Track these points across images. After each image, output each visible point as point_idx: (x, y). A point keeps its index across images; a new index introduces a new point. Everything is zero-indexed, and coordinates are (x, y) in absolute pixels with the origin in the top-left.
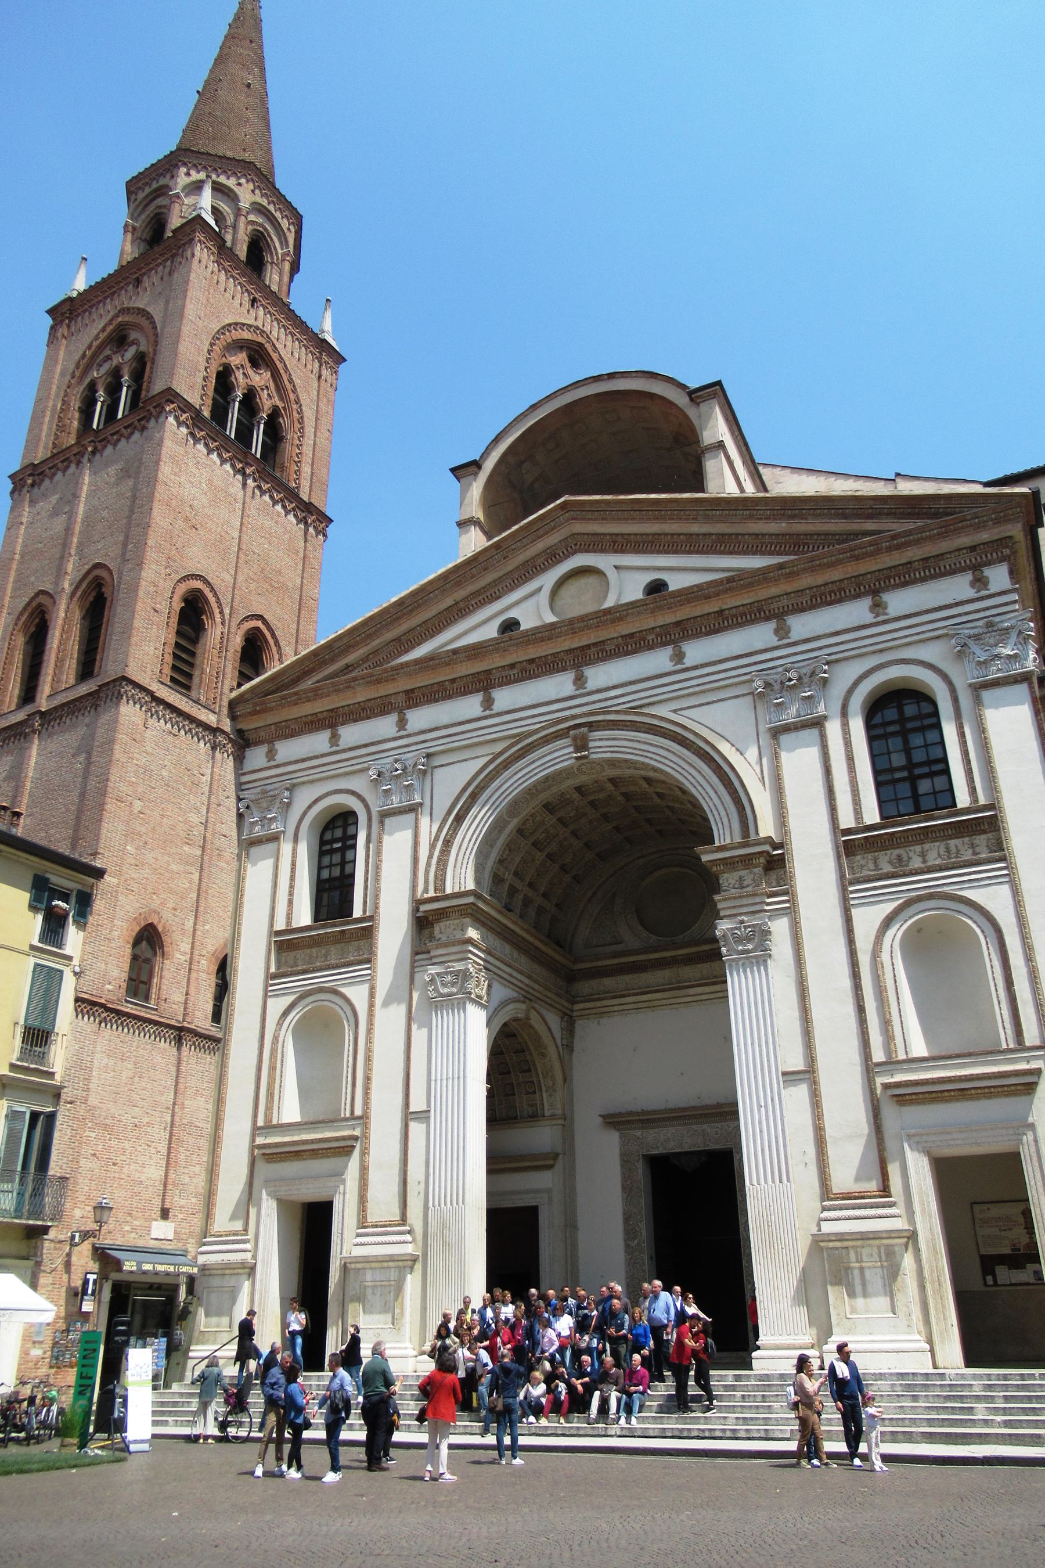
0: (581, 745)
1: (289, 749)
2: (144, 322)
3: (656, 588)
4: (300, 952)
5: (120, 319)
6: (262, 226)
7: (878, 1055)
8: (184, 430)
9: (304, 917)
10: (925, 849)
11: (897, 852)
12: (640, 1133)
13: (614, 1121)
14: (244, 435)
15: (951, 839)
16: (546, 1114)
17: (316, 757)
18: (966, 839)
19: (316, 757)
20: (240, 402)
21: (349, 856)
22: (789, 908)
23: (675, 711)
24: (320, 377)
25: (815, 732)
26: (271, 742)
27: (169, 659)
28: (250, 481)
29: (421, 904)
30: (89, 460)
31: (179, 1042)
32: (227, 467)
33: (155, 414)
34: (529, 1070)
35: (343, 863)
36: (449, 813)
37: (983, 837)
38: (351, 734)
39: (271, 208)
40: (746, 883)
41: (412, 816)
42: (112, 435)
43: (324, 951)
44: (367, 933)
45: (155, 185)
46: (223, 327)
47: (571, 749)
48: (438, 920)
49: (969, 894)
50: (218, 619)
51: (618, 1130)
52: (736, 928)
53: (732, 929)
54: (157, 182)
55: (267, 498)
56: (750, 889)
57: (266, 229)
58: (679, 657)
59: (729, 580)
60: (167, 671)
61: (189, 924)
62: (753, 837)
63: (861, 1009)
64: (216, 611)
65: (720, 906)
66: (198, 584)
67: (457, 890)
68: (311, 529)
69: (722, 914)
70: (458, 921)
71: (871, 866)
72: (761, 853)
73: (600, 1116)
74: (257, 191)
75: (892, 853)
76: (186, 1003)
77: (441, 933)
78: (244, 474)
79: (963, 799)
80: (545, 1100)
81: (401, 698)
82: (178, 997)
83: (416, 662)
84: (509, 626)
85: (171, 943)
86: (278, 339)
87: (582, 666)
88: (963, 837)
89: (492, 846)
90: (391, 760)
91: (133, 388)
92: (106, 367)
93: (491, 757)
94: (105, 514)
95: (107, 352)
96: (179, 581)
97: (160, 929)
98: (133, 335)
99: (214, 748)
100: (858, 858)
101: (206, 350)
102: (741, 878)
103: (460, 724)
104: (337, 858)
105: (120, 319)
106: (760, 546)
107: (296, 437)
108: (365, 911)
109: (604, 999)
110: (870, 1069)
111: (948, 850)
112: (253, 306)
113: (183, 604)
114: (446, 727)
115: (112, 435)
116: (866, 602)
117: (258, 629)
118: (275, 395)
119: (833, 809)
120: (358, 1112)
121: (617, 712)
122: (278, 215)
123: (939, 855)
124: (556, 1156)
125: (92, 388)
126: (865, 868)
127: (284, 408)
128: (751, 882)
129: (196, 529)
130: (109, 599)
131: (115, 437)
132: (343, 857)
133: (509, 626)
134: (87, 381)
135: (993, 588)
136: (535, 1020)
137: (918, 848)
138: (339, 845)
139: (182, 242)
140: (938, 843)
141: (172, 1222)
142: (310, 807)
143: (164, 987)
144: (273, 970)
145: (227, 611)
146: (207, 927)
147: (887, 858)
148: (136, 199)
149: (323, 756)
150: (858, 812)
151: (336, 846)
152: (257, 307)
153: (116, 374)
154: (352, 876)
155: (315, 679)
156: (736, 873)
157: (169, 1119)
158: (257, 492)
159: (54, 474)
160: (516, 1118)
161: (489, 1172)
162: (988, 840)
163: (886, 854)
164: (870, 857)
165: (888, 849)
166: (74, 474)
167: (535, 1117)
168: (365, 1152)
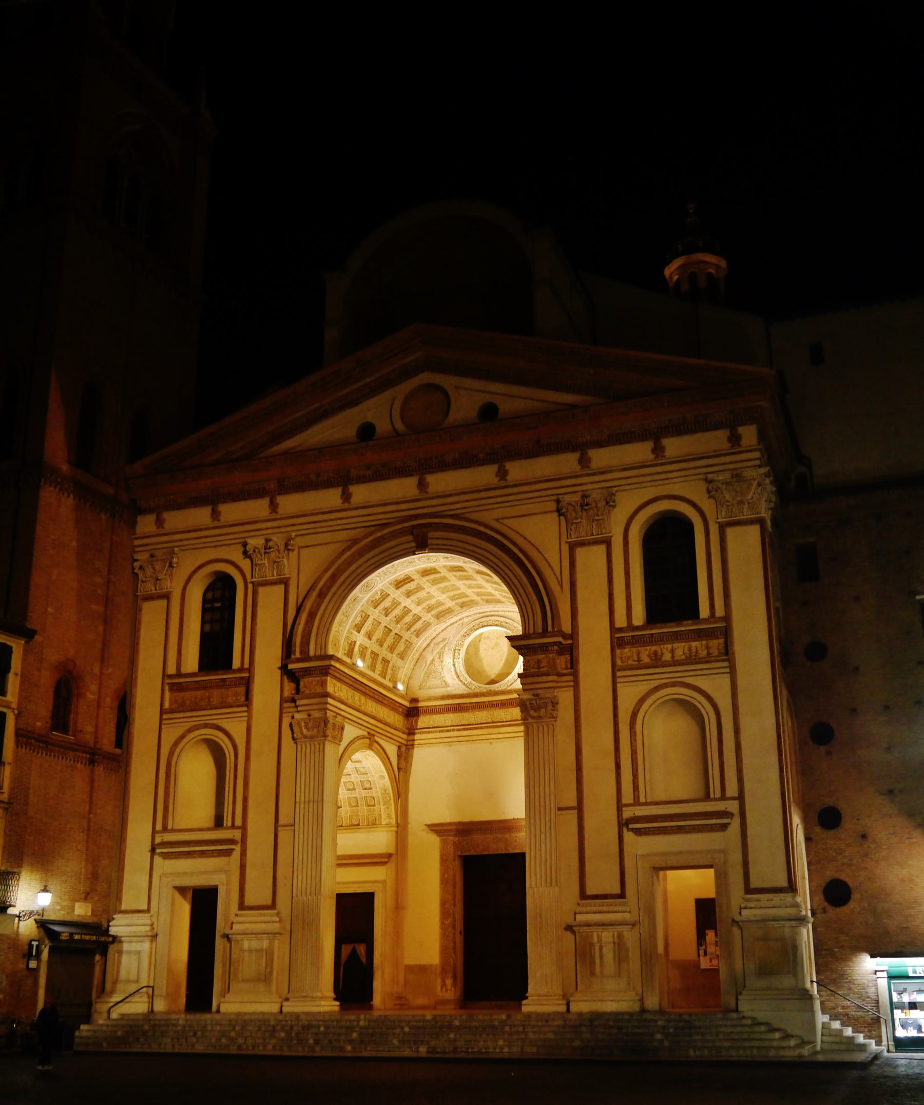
1: (175, 519)
3: (489, 412)
7: (627, 798)
9: (191, 663)
11: (654, 648)
13: (437, 829)
15: (693, 641)
17: (201, 530)
18: (704, 643)
22: (572, 686)
23: (497, 520)
26: (158, 511)
31: (92, 762)
40: (542, 665)
48: (304, 676)
49: (701, 682)
51: (439, 836)
52: (532, 699)
53: (530, 700)
56: (545, 669)
58: (502, 474)
61: (96, 669)
62: (550, 629)
63: (618, 766)
67: (318, 653)
71: (636, 658)
72: (555, 643)
77: (305, 687)
79: (704, 612)
81: (272, 485)
82: (90, 729)
84: (367, 432)
88: (702, 640)
100: (627, 650)
110: (620, 807)
111: (690, 648)
114: (312, 514)
116: (649, 445)
120: (238, 822)
121: (451, 516)
123: (684, 653)
124: (390, 856)
126: (631, 659)
133: (367, 432)
137: (669, 646)
138: (219, 605)
141: (90, 902)
144: (167, 705)
146: (110, 670)
147: (647, 653)
156: (536, 656)
157: (85, 825)
160: (358, 825)
165: (649, 646)
168: (243, 854)
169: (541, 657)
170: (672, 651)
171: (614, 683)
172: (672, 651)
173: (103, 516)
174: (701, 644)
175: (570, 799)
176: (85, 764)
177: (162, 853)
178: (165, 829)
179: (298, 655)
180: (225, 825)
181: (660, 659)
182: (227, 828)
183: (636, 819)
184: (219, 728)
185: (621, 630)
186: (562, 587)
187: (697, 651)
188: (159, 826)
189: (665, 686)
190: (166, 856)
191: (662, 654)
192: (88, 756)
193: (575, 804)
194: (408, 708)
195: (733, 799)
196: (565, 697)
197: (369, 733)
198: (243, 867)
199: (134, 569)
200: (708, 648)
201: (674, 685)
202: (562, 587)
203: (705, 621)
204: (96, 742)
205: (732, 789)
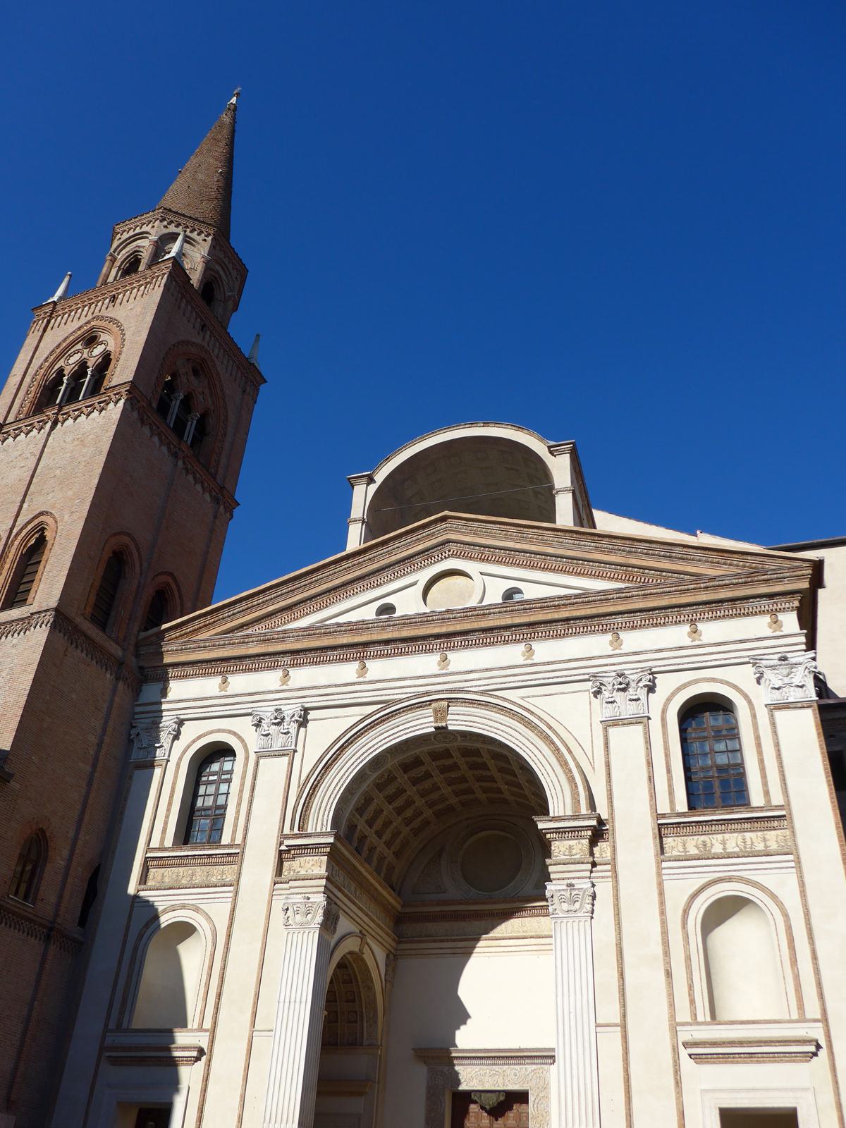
0: (441, 714)
2: (115, 328)
4: (169, 869)
5: (93, 323)
6: (217, 272)
7: (683, 1015)
8: (135, 414)
10: (725, 839)
12: (447, 1069)
14: (179, 428)
16: (364, 1044)
17: (206, 699)
19: (206, 699)
20: (181, 401)
21: (223, 788)
23: (522, 698)
24: (244, 391)
25: (640, 728)
27: (93, 598)
28: (180, 463)
29: (285, 838)
30: (52, 428)
31: (48, 938)
32: (164, 449)
33: (114, 399)
34: (353, 1001)
35: (217, 794)
36: (320, 760)
37: (773, 833)
38: (240, 682)
39: (226, 261)
40: (574, 852)
41: (286, 759)
42: (73, 411)
43: (190, 872)
44: (234, 857)
45: (138, 230)
46: (178, 343)
47: (432, 719)
50: (137, 570)
54: (140, 228)
55: (190, 478)
57: (220, 276)
59: (577, 596)
60: (89, 609)
61: (71, 834)
64: (137, 563)
65: (551, 869)
66: (126, 539)
67: (318, 830)
68: (222, 509)
69: (552, 876)
70: (317, 858)
71: (681, 850)
73: (413, 1049)
74: (218, 248)
75: (698, 839)
76: (58, 905)
78: (175, 455)
80: (365, 1029)
82: (53, 899)
83: (305, 629)
84: (388, 609)
85: (55, 848)
86: (217, 358)
87: (446, 651)
89: (352, 794)
90: (272, 709)
91: (96, 377)
92: (77, 357)
93: (363, 716)
94: (58, 472)
95: (79, 346)
96: (115, 535)
97: (48, 835)
98: (103, 337)
99: (117, 679)
101: (162, 357)
102: (570, 847)
103: (336, 686)
104: (212, 789)
105: (93, 323)
106: (601, 572)
107: (219, 434)
108: (233, 839)
109: (425, 942)
110: (674, 1026)
112: (202, 330)
113: (111, 555)
115: (73, 411)
117: (168, 584)
118: (209, 400)
119: (653, 796)
121: (475, 693)
122: (230, 266)
123: (737, 846)
125: (61, 371)
127: (214, 411)
128: (579, 851)
129: (132, 496)
130: (49, 546)
131: (76, 413)
132: (218, 789)
134: (56, 367)
135: (786, 631)
136: (367, 956)
137: (720, 837)
138: (215, 778)
139: (156, 274)
140: (736, 834)
142: (194, 741)
143: (42, 888)
145: (145, 565)
147: (694, 843)
148: (120, 238)
149: (211, 698)
150: (672, 802)
151: (211, 778)
152: (206, 331)
153: (83, 365)
154: (224, 807)
155: (213, 632)
156: (566, 842)
158: (184, 472)
159: (17, 436)
161: (319, 1093)
162: (777, 836)
163: (693, 839)
164: (679, 840)
166: (35, 437)
167: (354, 1043)
169: (573, 843)
170: (724, 843)
171: (659, 875)
172: (724, 843)
173: (109, 676)
174: (757, 836)
175: (611, 1013)
176: (40, 939)
177: (111, 1057)
178: (119, 1027)
179: (296, 831)
180: (190, 1026)
181: (710, 851)
182: (192, 1030)
183: (696, 1044)
184: (197, 910)
185: (663, 816)
186: (594, 768)
187: (752, 843)
188: (112, 1025)
189: (719, 880)
190: (115, 1061)
191: (712, 845)
192: (45, 930)
193: (618, 1020)
194: (400, 913)
195: (815, 1021)
196: (604, 889)
197: (361, 932)
198: (206, 1080)
199: (130, 735)
200: (765, 840)
201: (730, 879)
202: (594, 768)
203: (760, 809)
204: (56, 915)
205: (813, 1010)
